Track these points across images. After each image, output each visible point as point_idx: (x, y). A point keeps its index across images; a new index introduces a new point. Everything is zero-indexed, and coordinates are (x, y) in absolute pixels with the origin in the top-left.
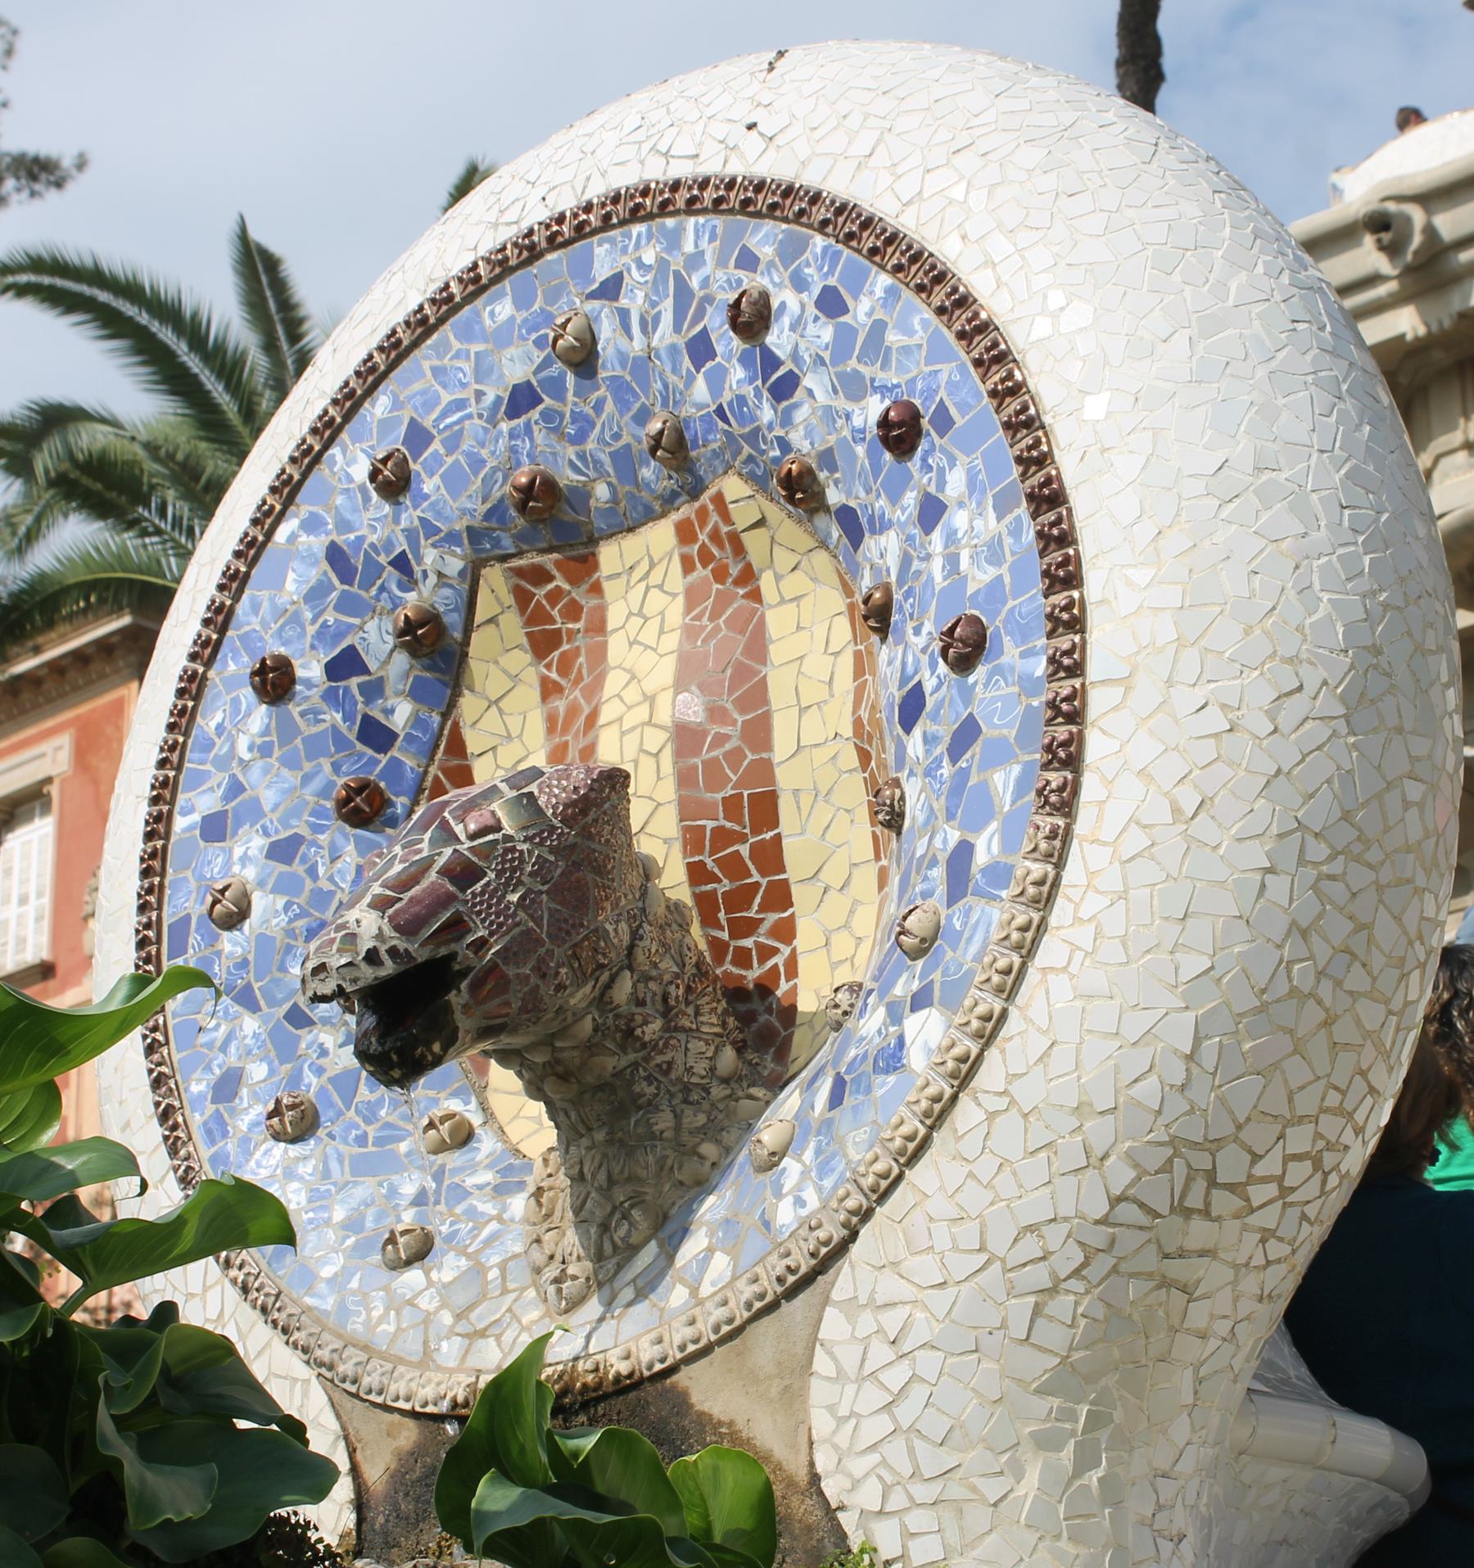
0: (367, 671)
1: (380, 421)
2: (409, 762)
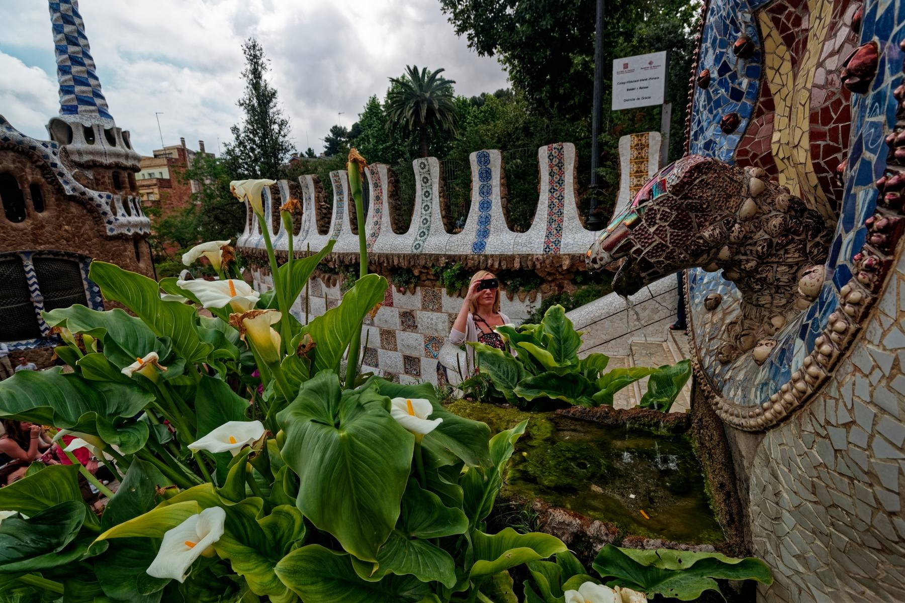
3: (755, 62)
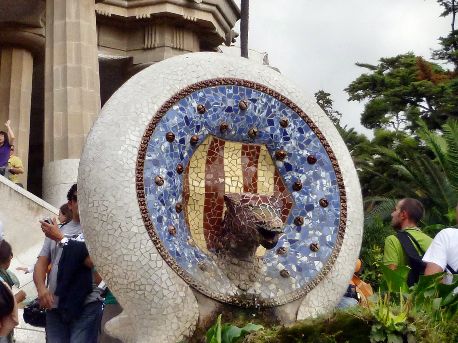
0: (184, 144)
1: (200, 97)
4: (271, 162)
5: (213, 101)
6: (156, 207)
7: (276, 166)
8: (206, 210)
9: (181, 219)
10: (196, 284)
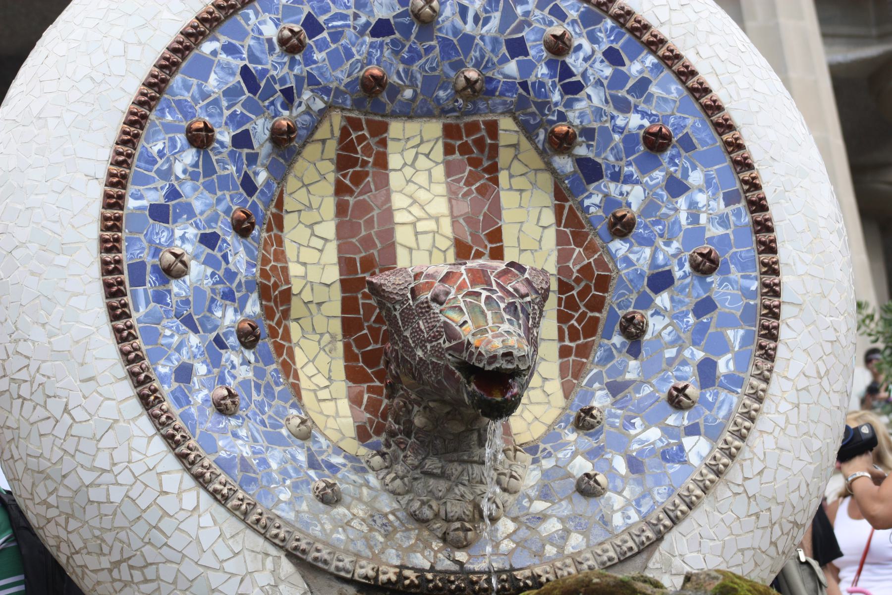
0: (253, 148)
1: (284, 6)
2: (261, 206)
3: (283, 157)
4: (537, 162)
5: (326, 10)
6: (170, 340)
7: (553, 171)
8: (349, 327)
9: (261, 365)
10: (303, 545)
